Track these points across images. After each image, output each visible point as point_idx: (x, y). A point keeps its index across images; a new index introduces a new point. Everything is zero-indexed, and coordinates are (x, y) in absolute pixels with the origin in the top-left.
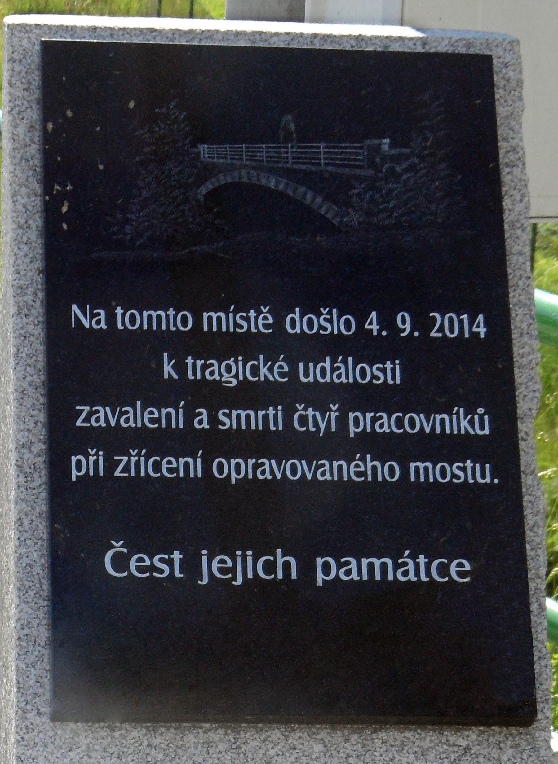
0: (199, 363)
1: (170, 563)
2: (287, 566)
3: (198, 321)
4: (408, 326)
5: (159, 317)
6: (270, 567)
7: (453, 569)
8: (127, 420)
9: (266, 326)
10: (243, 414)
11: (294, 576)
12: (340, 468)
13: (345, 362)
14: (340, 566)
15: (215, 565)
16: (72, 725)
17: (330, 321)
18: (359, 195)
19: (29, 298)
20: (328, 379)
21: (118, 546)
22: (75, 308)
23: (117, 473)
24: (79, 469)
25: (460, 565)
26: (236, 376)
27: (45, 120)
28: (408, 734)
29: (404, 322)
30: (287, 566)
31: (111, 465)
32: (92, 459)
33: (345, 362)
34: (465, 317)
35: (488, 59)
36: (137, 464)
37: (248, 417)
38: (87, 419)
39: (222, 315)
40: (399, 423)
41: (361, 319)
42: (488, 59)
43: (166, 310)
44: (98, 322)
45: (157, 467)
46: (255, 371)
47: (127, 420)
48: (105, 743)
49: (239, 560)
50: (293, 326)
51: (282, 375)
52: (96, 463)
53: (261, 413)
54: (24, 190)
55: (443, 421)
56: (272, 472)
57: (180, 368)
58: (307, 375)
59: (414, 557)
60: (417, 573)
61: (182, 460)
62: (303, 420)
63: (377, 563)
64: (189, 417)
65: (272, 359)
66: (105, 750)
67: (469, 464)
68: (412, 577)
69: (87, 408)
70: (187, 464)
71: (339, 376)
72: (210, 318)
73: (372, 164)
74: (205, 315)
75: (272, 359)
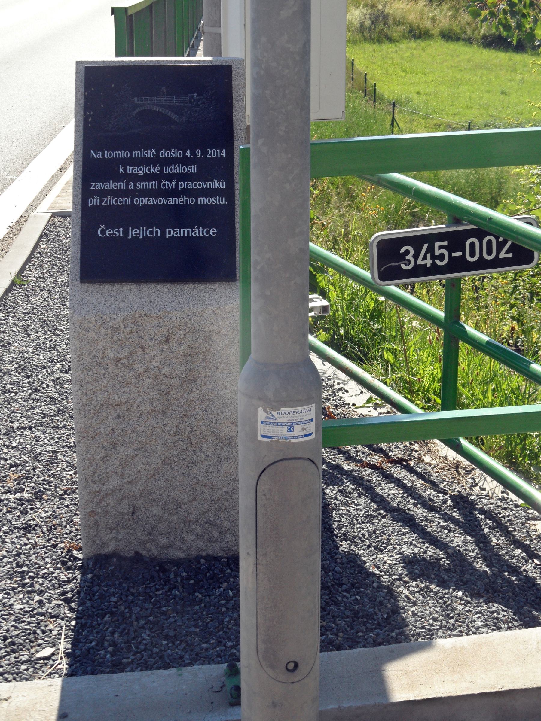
0: (131, 168)
1: (119, 232)
2: (157, 232)
3: (131, 154)
4: (200, 154)
5: (119, 153)
6: (151, 232)
7: (211, 232)
8: (107, 187)
9: (153, 155)
10: (145, 184)
11: (159, 235)
12: (176, 200)
13: (179, 166)
14: (174, 231)
15: (134, 232)
16: (87, 284)
17: (174, 153)
18: (186, 112)
19: (79, 149)
20: (173, 172)
21: (103, 227)
22: (92, 151)
23: (103, 204)
24: (91, 203)
25: (213, 230)
26: (143, 172)
27: (85, 92)
28: (196, 285)
29: (198, 152)
30: (157, 232)
31: (102, 202)
32: (95, 199)
33: (179, 166)
34: (219, 150)
35: (230, 66)
36: (110, 201)
37: (146, 184)
38: (94, 187)
39: (139, 152)
40: (196, 185)
41: (185, 152)
42: (230, 66)
43: (121, 151)
44: (99, 156)
45: (116, 201)
46: (149, 170)
47: (107, 187)
48: (97, 290)
49: (141, 230)
50: (162, 155)
51: (158, 171)
52: (97, 201)
53: (150, 183)
54: (79, 114)
55: (210, 184)
56: (153, 202)
57: (125, 170)
58: (166, 171)
59: (198, 228)
60: (199, 233)
61: (124, 199)
62: (164, 185)
63: (186, 230)
64: (127, 185)
65: (155, 166)
66: (97, 292)
67: (218, 198)
68: (197, 234)
69: (94, 183)
70: (126, 200)
71: (176, 171)
72: (135, 153)
73: (190, 102)
74: (134, 152)
75: (155, 166)
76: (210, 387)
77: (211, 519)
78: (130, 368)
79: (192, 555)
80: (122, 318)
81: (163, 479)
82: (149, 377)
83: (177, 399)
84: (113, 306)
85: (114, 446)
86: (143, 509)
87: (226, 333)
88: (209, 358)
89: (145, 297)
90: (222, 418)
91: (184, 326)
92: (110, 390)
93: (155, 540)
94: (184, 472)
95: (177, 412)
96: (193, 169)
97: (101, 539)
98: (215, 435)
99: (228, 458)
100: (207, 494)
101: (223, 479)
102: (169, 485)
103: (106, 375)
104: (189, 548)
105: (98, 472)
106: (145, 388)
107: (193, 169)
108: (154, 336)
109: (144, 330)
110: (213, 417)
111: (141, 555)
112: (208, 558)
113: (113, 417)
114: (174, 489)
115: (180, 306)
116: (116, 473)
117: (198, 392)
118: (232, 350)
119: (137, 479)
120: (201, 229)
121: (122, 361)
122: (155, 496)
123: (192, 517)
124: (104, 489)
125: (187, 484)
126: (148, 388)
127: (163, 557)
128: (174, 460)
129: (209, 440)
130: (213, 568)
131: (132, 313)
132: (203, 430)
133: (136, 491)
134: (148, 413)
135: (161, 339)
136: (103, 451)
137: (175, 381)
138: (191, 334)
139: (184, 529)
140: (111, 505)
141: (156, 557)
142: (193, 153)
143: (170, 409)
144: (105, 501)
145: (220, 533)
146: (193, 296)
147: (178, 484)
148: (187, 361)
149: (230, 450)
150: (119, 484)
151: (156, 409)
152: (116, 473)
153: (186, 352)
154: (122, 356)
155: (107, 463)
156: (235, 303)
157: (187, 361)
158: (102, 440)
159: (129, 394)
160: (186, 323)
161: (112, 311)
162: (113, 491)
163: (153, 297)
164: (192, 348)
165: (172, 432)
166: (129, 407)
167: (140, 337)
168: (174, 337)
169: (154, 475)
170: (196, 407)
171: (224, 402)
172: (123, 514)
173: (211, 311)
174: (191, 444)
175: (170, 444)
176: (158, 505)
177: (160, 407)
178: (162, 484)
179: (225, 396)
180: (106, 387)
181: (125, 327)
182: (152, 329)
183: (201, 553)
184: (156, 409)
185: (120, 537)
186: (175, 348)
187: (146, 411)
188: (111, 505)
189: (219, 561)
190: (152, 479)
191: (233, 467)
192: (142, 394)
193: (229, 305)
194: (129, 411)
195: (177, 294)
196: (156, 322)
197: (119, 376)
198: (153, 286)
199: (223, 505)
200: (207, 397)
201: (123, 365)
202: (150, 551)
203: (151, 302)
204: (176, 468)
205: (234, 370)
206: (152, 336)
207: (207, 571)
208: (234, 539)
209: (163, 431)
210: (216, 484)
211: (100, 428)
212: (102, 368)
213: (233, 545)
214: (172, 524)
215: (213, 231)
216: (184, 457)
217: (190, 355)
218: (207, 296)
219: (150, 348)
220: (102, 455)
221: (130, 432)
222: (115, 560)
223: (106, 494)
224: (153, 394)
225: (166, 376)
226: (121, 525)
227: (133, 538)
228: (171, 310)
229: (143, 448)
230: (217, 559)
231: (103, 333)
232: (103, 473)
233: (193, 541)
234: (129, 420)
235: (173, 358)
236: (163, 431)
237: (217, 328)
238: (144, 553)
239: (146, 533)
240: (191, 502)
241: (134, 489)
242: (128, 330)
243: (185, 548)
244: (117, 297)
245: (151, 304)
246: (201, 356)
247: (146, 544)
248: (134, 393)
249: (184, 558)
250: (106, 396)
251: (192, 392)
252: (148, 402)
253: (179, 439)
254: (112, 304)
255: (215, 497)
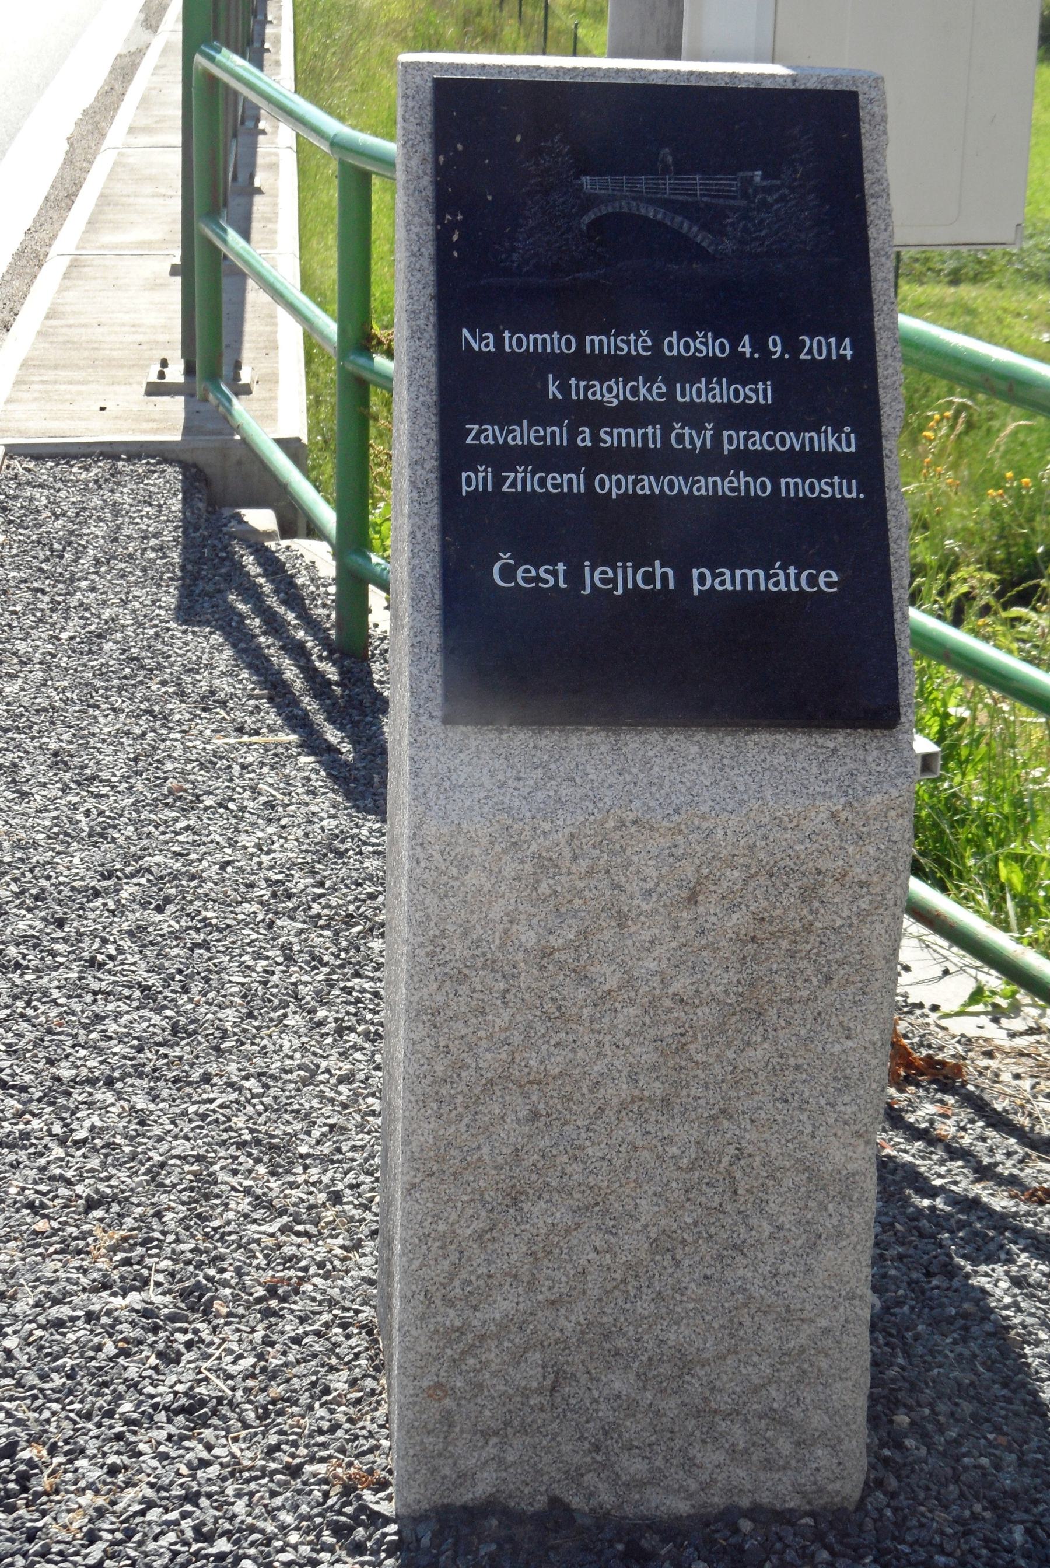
0: (582, 384)
1: (555, 574)
2: (665, 577)
3: (581, 344)
4: (779, 349)
5: (544, 340)
6: (649, 578)
7: (822, 579)
8: (514, 438)
9: (645, 349)
10: (624, 432)
11: (671, 586)
12: (715, 483)
13: (720, 383)
14: (715, 576)
15: (597, 576)
16: (462, 728)
17: (706, 344)
18: (732, 224)
19: (421, 322)
20: (703, 399)
21: (506, 558)
22: (465, 331)
23: (505, 489)
24: (469, 484)
25: (828, 576)
26: (617, 396)
27: (437, 153)
28: (779, 737)
29: (775, 345)
30: (665, 577)
31: (499, 481)
32: (481, 475)
33: (720, 383)
34: (833, 340)
35: (854, 95)
36: (524, 480)
37: (628, 435)
38: (477, 437)
39: (604, 338)
40: (771, 441)
41: (735, 342)
42: (854, 95)
43: (551, 334)
44: (487, 345)
45: (542, 482)
46: (635, 391)
47: (514, 438)
48: (493, 745)
49: (620, 571)
50: (671, 349)
51: (660, 395)
52: (485, 479)
53: (640, 432)
54: (417, 220)
55: (811, 439)
56: (651, 488)
57: (564, 388)
58: (683, 395)
59: (784, 568)
60: (788, 583)
61: (566, 477)
62: (680, 438)
63: (750, 574)
64: (573, 435)
65: (650, 380)
66: (493, 751)
67: (836, 480)
68: (783, 587)
69: (476, 427)
70: (570, 480)
71: (714, 397)
72: (592, 342)
73: (745, 195)
74: (588, 338)
75: (650, 380)
76: (803, 1032)
77: (775, 1405)
78: (583, 978)
79: (712, 1505)
80: (568, 830)
81: (648, 1294)
82: (632, 1002)
83: (705, 1065)
84: (540, 795)
85: (515, 1201)
86: (584, 1379)
87: (863, 877)
88: (808, 947)
89: (634, 771)
90: (831, 1121)
91: (744, 855)
92: (517, 1039)
93: (612, 1466)
94: (709, 1273)
95: (702, 1102)
96: (761, 393)
97: (455, 1464)
98: (807, 1169)
99: (840, 1234)
100: (769, 1338)
101: (821, 1293)
102: (664, 1310)
103: (510, 996)
104: (704, 1487)
105: (464, 1275)
106: (620, 1035)
107: (761, 393)
108: (657, 885)
109: (627, 867)
110: (804, 1117)
111: (567, 1508)
112: (754, 1512)
113: (520, 1115)
114: (677, 1323)
115: (738, 797)
116: (515, 1276)
117: (766, 1046)
118: (878, 926)
119: (575, 1293)
120: (792, 571)
121: (556, 955)
122: (621, 1343)
123: (722, 1401)
124: (475, 1323)
125: (715, 1308)
126: (628, 1034)
127: (629, 1511)
128: (684, 1240)
129: (787, 1183)
130: (778, 1546)
131: (598, 816)
132: (774, 1154)
133: (569, 1326)
134: (623, 1106)
135: (676, 891)
136: (483, 1214)
137: (706, 1015)
138: (763, 880)
139: (697, 1433)
140: (493, 1367)
141: (608, 1513)
142: (760, 345)
143: (684, 1092)
144: (475, 1356)
145: (798, 1444)
146: (772, 769)
147: (691, 1306)
148: (744, 958)
149: (846, 1211)
150: (520, 1307)
151: (646, 1094)
152: (515, 1276)
153: (743, 932)
154: (561, 941)
155: (490, 1246)
156: (895, 793)
157: (744, 958)
158: (482, 1183)
159: (573, 1050)
160: (752, 848)
161: (538, 810)
162: (503, 1327)
163: (656, 769)
164: (763, 919)
165: (685, 1161)
166: (569, 1088)
167: (617, 887)
168: (712, 888)
169: (624, 1281)
170: (757, 1088)
171: (839, 1074)
172: (525, 1393)
173: (824, 816)
174: (735, 1193)
175: (675, 1195)
176: (626, 1368)
177: (658, 1089)
178: (644, 1307)
179: (843, 1057)
180: (506, 1029)
181: (575, 858)
182: (650, 863)
183: (736, 1498)
184: (646, 1094)
185: (511, 1459)
186: (714, 919)
187: (615, 1101)
188: (493, 1367)
189: (793, 1525)
190: (617, 1293)
191: (851, 1258)
192: (608, 1050)
193: (879, 798)
194: (568, 1098)
195: (726, 761)
196: (665, 842)
197: (546, 999)
198: (654, 736)
199: (811, 1365)
200: (792, 1061)
201: (561, 965)
202: (592, 1494)
203: (651, 784)
204: (687, 1262)
205: (878, 984)
206: (650, 885)
207: (764, 1556)
208: (835, 1461)
209: (659, 1157)
210: (799, 1306)
211: (479, 1148)
212: (499, 976)
213: (832, 1477)
214: (664, 1420)
215: (827, 579)
216: (712, 1230)
217: (753, 939)
218: (815, 770)
219: (642, 918)
220: (479, 1225)
221: (565, 1159)
222: (494, 1522)
223: (482, 1337)
224: (639, 1050)
225: (682, 1001)
226: (516, 1423)
227: (548, 1459)
228: (712, 808)
229: (597, 1204)
230: (786, 1517)
231: (508, 872)
232: (478, 1277)
233: (718, 1466)
234: (564, 1124)
235: (705, 948)
236: (659, 1157)
237: (840, 863)
238: (576, 1502)
239: (587, 1445)
240: (723, 1357)
241: (562, 1322)
242: (584, 865)
243: (694, 1486)
244: (553, 766)
245: (653, 789)
246: (785, 944)
247: (582, 1475)
248: (586, 1047)
249: (689, 1516)
250: (504, 1056)
251: (748, 1044)
252: (624, 1074)
253: (700, 1180)
254: (537, 788)
255: (792, 1344)
